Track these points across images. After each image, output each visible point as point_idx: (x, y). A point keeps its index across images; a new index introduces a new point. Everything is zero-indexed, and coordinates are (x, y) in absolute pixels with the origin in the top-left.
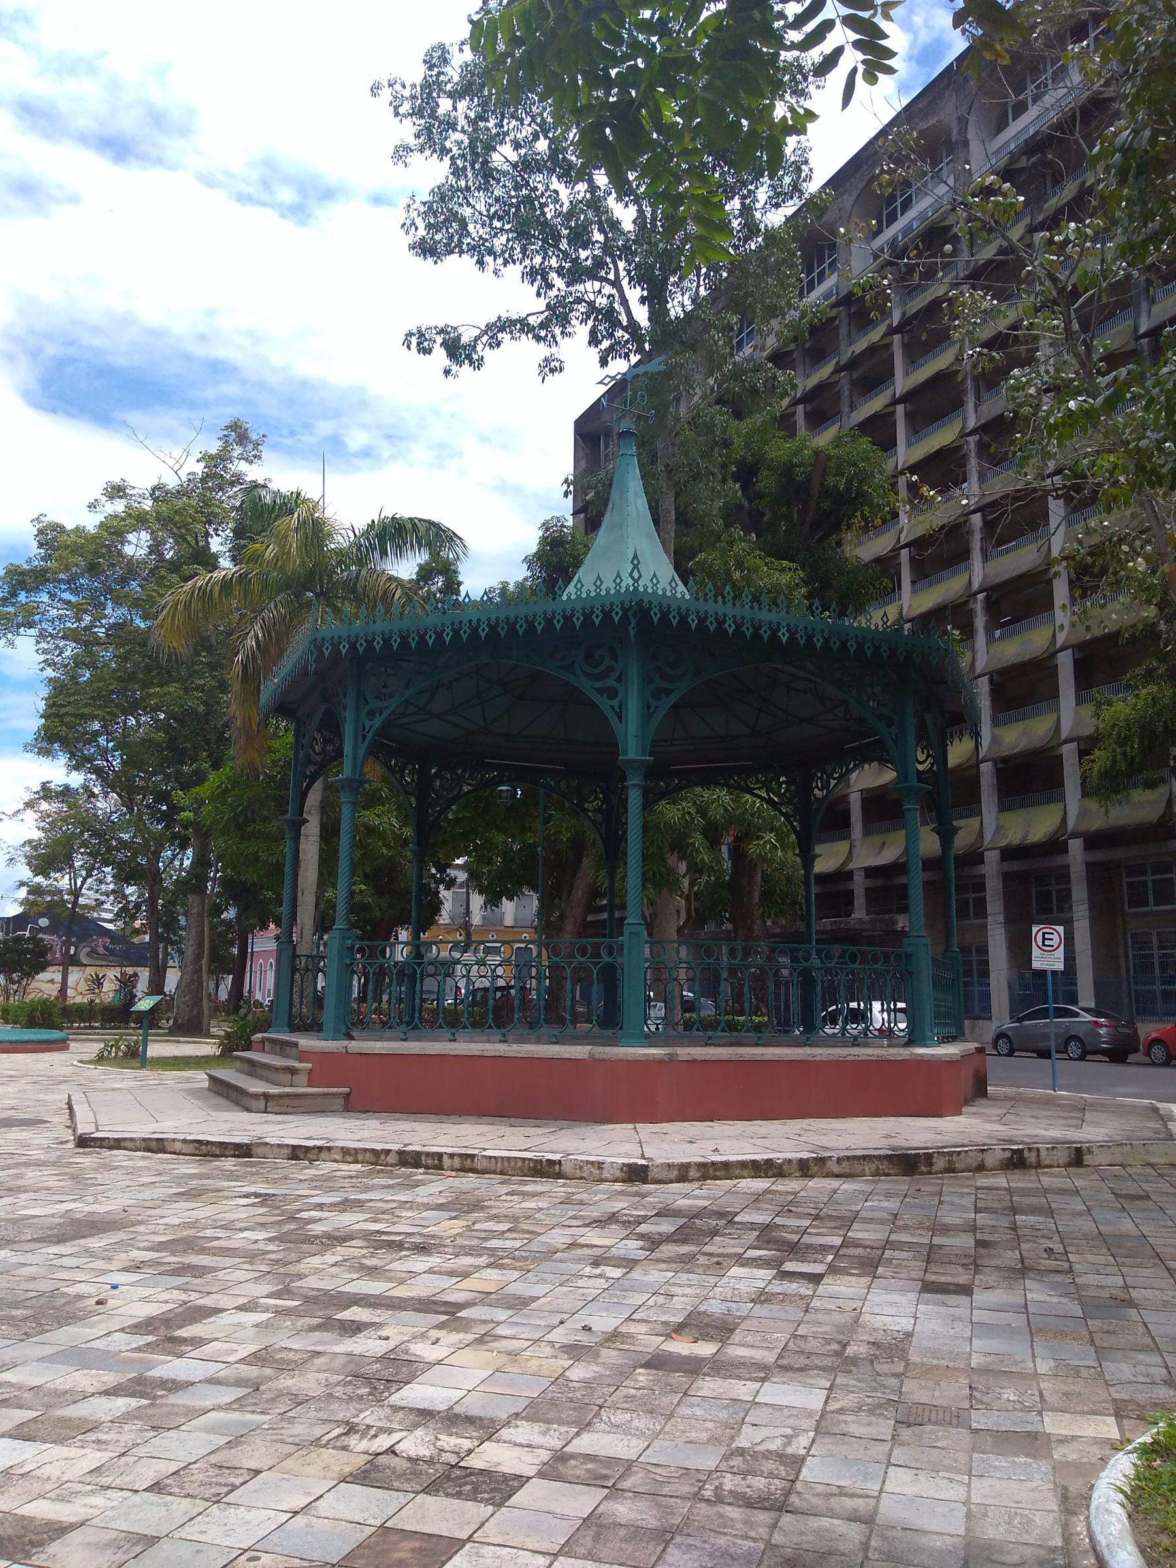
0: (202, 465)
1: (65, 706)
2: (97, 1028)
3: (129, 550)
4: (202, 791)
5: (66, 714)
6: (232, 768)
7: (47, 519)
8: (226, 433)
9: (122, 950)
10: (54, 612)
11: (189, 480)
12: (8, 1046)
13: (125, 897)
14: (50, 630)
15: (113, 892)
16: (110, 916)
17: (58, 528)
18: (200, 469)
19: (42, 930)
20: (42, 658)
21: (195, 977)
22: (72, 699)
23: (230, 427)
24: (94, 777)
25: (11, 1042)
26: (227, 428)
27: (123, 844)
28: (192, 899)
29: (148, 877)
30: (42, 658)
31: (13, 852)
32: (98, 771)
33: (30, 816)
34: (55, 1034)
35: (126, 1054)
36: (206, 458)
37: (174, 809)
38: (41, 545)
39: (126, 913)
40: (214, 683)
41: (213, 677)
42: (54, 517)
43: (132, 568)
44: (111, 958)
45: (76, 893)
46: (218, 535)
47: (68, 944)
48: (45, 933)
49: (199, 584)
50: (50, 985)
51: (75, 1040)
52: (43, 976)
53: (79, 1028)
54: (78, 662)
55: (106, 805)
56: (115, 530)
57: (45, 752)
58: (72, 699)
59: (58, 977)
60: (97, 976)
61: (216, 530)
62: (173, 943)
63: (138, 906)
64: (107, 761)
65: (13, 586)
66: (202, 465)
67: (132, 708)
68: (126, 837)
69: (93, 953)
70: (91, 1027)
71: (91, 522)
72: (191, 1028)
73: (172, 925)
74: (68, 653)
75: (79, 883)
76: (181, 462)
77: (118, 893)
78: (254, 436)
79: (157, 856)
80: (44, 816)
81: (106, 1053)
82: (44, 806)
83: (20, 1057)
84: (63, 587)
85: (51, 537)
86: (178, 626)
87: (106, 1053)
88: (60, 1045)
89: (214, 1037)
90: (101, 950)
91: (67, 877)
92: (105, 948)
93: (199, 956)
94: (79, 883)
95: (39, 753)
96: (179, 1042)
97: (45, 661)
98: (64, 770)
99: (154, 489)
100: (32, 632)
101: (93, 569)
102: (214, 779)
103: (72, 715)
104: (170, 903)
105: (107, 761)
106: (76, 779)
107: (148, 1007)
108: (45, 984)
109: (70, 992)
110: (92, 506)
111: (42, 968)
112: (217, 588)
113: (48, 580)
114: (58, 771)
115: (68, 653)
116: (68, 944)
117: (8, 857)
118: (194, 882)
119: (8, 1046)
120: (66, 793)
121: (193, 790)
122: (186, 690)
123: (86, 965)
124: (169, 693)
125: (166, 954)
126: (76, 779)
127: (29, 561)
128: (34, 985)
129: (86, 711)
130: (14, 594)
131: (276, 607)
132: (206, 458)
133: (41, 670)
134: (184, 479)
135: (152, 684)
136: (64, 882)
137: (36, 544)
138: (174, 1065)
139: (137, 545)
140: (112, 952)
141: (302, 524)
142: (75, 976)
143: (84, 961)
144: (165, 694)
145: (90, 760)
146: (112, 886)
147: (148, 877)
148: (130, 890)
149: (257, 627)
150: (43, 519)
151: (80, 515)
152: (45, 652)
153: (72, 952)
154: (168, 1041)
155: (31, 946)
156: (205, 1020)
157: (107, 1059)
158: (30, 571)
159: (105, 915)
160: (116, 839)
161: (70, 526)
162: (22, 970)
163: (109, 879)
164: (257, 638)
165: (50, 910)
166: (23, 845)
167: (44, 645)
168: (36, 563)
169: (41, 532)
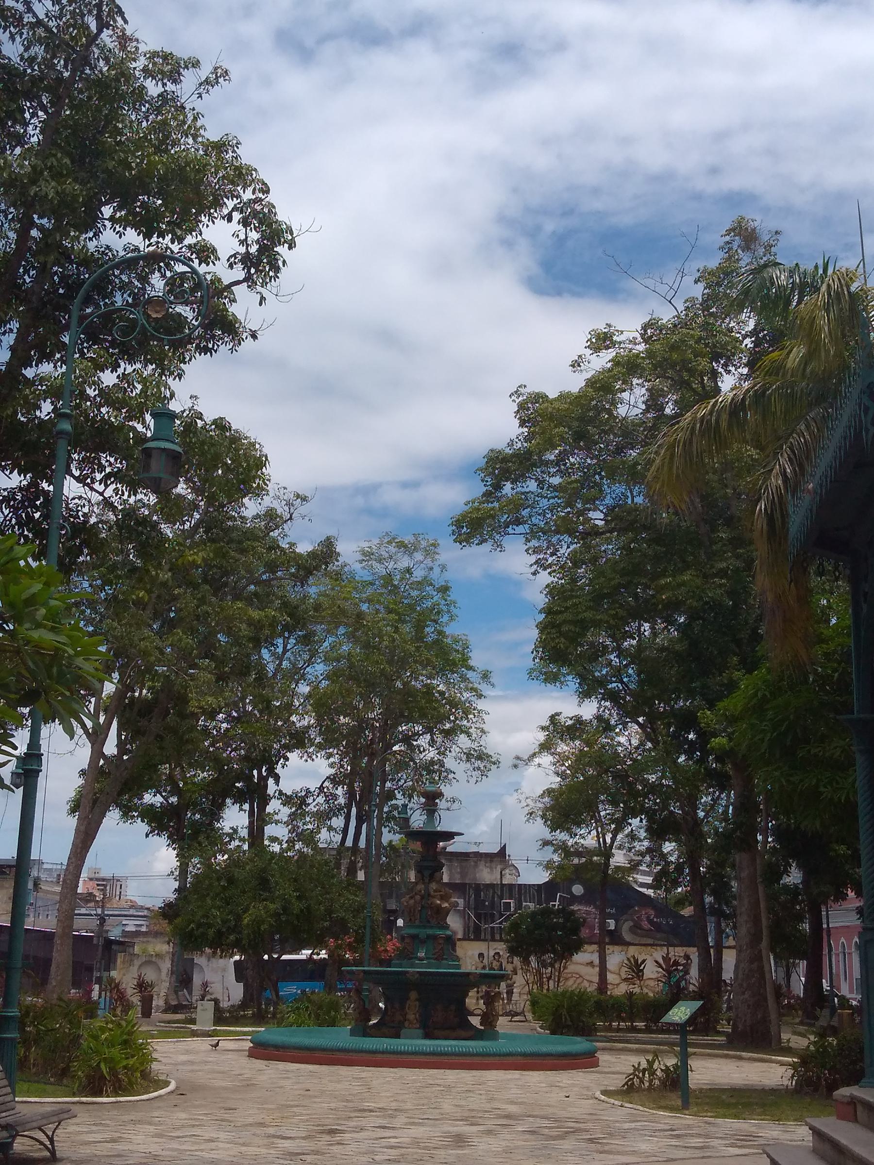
0: (701, 286)
1: (561, 612)
2: (639, 1031)
3: (622, 411)
4: (733, 704)
5: (565, 622)
6: (769, 671)
7: (529, 390)
8: (728, 238)
9: (668, 927)
10: (544, 503)
11: (687, 308)
12: (520, 1060)
13: (663, 856)
14: (542, 524)
15: (649, 850)
16: (649, 880)
17: (539, 398)
18: (698, 291)
19: (574, 899)
20: (533, 558)
21: (755, 966)
22: (570, 603)
23: (733, 230)
24: (608, 704)
25: (524, 1055)
26: (729, 232)
27: (654, 789)
28: (738, 857)
29: (686, 829)
30: (533, 558)
31: (532, 804)
32: (613, 697)
33: (546, 759)
34: (578, 1044)
35: (663, 1083)
36: (704, 276)
37: (704, 736)
38: (522, 424)
39: (665, 878)
40: (739, 564)
41: (738, 557)
42: (534, 387)
43: (629, 432)
44: (659, 935)
45: (606, 852)
46: (729, 372)
47: (604, 916)
48: (580, 903)
49: (699, 415)
50: (589, 969)
51: (604, 1049)
52: (579, 957)
53: (618, 1030)
54: (576, 561)
55: (628, 738)
56: (603, 387)
57: (552, 678)
58: (570, 603)
59: (595, 958)
60: (636, 961)
61: (725, 366)
62: (727, 917)
63: (679, 868)
64: (622, 682)
65: (496, 477)
66: (701, 286)
67: (645, 611)
68: (652, 778)
69: (636, 928)
70: (635, 1030)
71: (575, 383)
72: (755, 1038)
73: (721, 891)
74: (564, 551)
75: (608, 840)
76: (675, 287)
77: (654, 851)
78: (765, 238)
79: (692, 802)
80: (562, 758)
81: (636, 1081)
82: (562, 747)
83: (535, 1078)
84: (552, 470)
85: (535, 411)
86: (678, 476)
87: (636, 1081)
88: (585, 1061)
89: (787, 1051)
90: (645, 925)
91: (594, 833)
92: (651, 922)
93: (756, 938)
94: (608, 840)
95: (546, 681)
96: (740, 1058)
97: (536, 562)
98: (575, 699)
99: (645, 328)
100: (520, 529)
101: (581, 438)
102: (747, 685)
103: (570, 622)
104: (718, 865)
105: (622, 682)
106: (589, 710)
107: (685, 1018)
108: (582, 968)
109: (611, 978)
110: (576, 364)
111: (577, 947)
112: (725, 417)
113: (534, 465)
114: (569, 704)
115: (564, 551)
116: (604, 916)
117: (527, 810)
118: (739, 837)
119: (520, 1060)
120: (575, 729)
121: (721, 705)
122: (705, 576)
123: (629, 944)
124: (683, 584)
125: (720, 932)
126: (589, 710)
127: (511, 444)
128: (571, 968)
129: (588, 615)
130: (498, 487)
131: (808, 427)
132: (704, 276)
133: (534, 574)
134: (681, 307)
135: (663, 574)
136: (588, 838)
137: (517, 422)
138: (728, 1106)
139: (632, 402)
140: (658, 927)
141: (836, 297)
142: (616, 958)
143: (627, 937)
144: (679, 585)
145: (601, 683)
146: (646, 843)
147: (686, 829)
148: (668, 847)
149: (783, 460)
150: (522, 390)
151: (560, 380)
152: (537, 550)
153: (612, 927)
154: (726, 1056)
155: (561, 920)
156: (773, 1030)
157: (639, 1090)
158: (513, 455)
159: (642, 879)
160: (641, 783)
161: (552, 394)
162: (554, 951)
163: (643, 834)
164: (784, 474)
165: (578, 874)
166: (542, 796)
167: (534, 543)
168: (519, 445)
169: (522, 407)
